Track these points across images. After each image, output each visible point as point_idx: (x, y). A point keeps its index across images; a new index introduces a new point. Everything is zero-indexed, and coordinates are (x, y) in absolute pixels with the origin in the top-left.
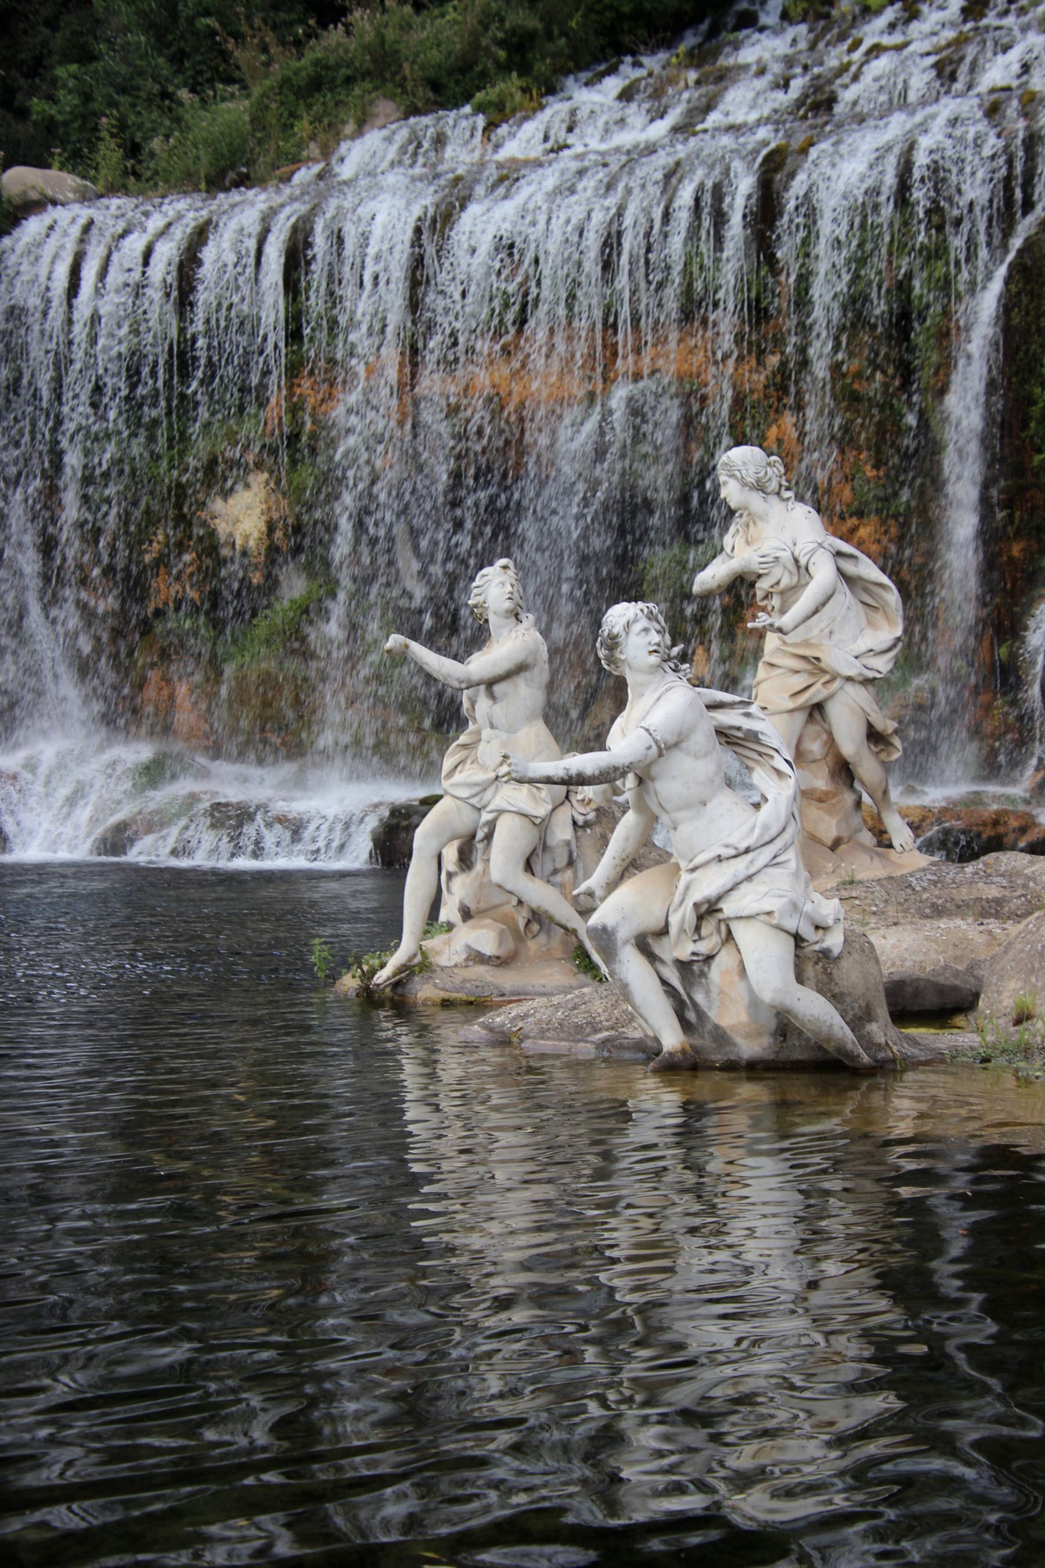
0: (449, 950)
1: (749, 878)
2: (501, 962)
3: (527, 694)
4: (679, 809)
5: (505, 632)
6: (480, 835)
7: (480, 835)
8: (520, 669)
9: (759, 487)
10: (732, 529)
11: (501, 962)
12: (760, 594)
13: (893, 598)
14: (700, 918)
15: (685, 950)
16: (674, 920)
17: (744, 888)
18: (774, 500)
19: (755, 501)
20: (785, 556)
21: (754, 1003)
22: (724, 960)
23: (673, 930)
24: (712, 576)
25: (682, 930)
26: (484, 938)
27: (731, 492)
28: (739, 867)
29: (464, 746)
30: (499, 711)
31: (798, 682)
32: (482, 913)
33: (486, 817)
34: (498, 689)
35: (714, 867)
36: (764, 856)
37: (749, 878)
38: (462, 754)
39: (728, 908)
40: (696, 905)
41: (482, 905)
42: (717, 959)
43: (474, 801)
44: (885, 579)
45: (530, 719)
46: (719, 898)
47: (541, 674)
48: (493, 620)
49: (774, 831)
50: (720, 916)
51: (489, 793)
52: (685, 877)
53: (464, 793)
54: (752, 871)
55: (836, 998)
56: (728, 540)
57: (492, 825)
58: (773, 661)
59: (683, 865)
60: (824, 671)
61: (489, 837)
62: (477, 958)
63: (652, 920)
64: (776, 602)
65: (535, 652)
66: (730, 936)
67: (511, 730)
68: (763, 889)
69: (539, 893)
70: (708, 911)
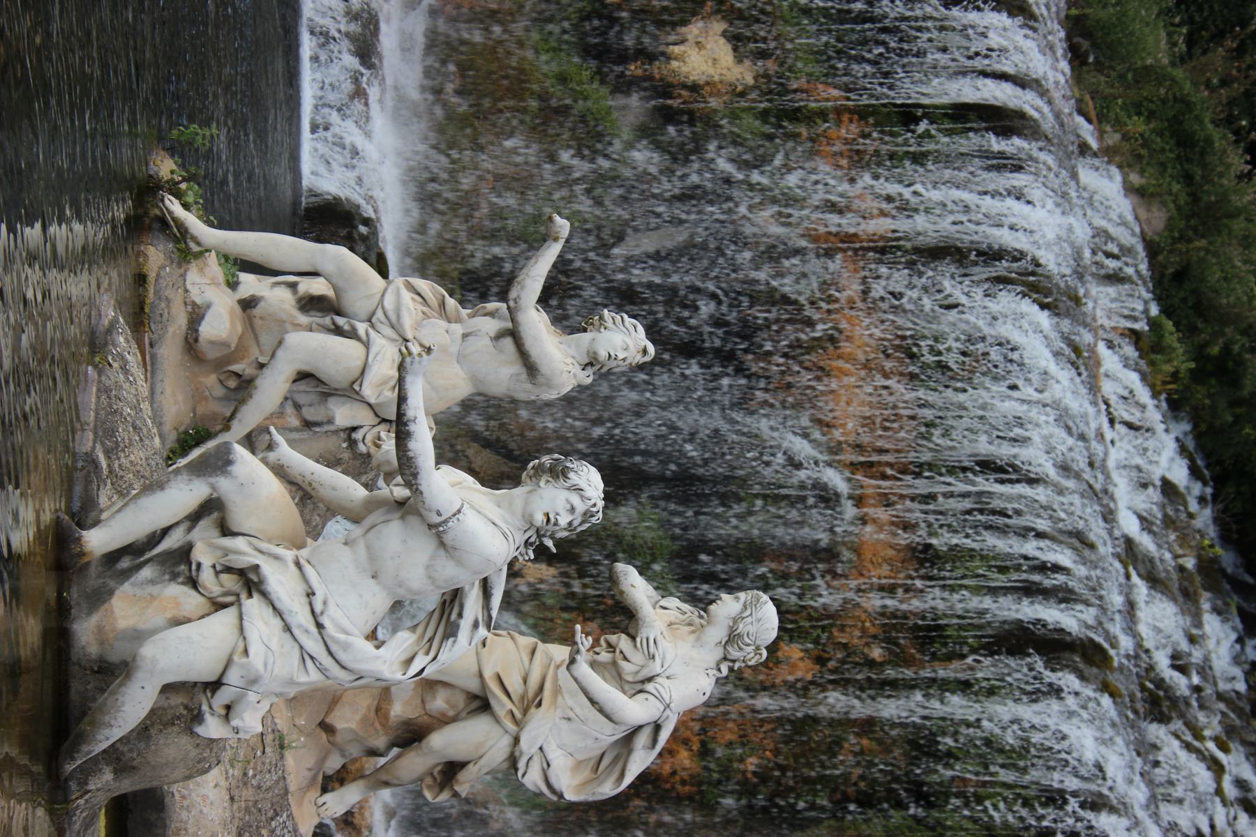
0: (204, 283)
1: (288, 629)
2: (191, 343)
3: (502, 375)
4: (368, 547)
5: (572, 351)
6: (341, 321)
7: (341, 321)
8: (531, 368)
9: (733, 637)
10: (686, 607)
11: (191, 343)
12: (613, 638)
13: (608, 789)
14: (241, 573)
15: (203, 555)
16: (239, 543)
17: (277, 622)
18: (719, 653)
19: (717, 633)
20: (656, 667)
21: (139, 636)
22: (191, 601)
23: (227, 542)
24: (636, 586)
25: (227, 552)
26: (220, 324)
27: (727, 606)
29: (443, 304)
30: (482, 343)
31: (514, 684)
32: (250, 323)
33: (362, 328)
34: (508, 342)
35: (301, 588)
36: (313, 645)
37: (288, 629)
38: (434, 302)
39: (253, 606)
40: (257, 567)
41: (258, 322)
42: (193, 593)
43: (380, 314)
44: (629, 779)
45: (474, 379)
46: (265, 595)
47: (524, 391)
48: (586, 337)
49: (342, 656)
50: (243, 596)
51: (388, 331)
52: (289, 555)
53: (389, 303)
54: (296, 632)
55: (144, 731)
56: (673, 602)
57: (352, 334)
59: (304, 553)
60: (525, 712)
61: (338, 331)
62: (196, 315)
63: (240, 516)
64: (605, 656)
65: (549, 385)
66: (219, 606)
67: (461, 358)
68: (274, 645)
69: (272, 388)
70: (251, 581)
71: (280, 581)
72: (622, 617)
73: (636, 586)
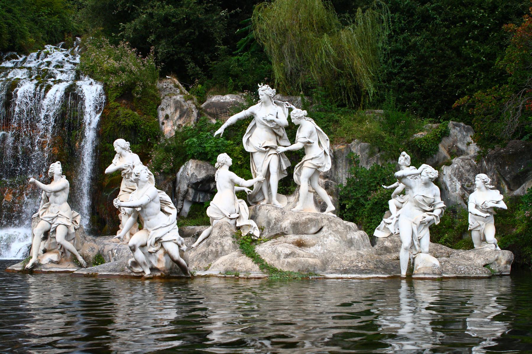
2: (58, 263)
3: (65, 196)
5: (59, 179)
6: (51, 230)
7: (51, 230)
8: (63, 189)
11: (58, 263)
12: (122, 174)
15: (152, 249)
19: (124, 152)
23: (148, 245)
24: (110, 169)
26: (54, 257)
27: (117, 149)
28: (167, 229)
33: (53, 226)
38: (44, 210)
41: (50, 249)
43: (50, 222)
45: (65, 202)
46: (162, 237)
47: (68, 190)
48: (55, 176)
51: (54, 220)
53: (48, 219)
56: (114, 161)
58: (125, 190)
61: (55, 231)
62: (52, 262)
63: (143, 242)
64: (127, 176)
65: (67, 185)
66: (162, 245)
69: (69, 245)
70: (158, 240)
71: (158, 234)
72: (119, 172)
73: (110, 169)
